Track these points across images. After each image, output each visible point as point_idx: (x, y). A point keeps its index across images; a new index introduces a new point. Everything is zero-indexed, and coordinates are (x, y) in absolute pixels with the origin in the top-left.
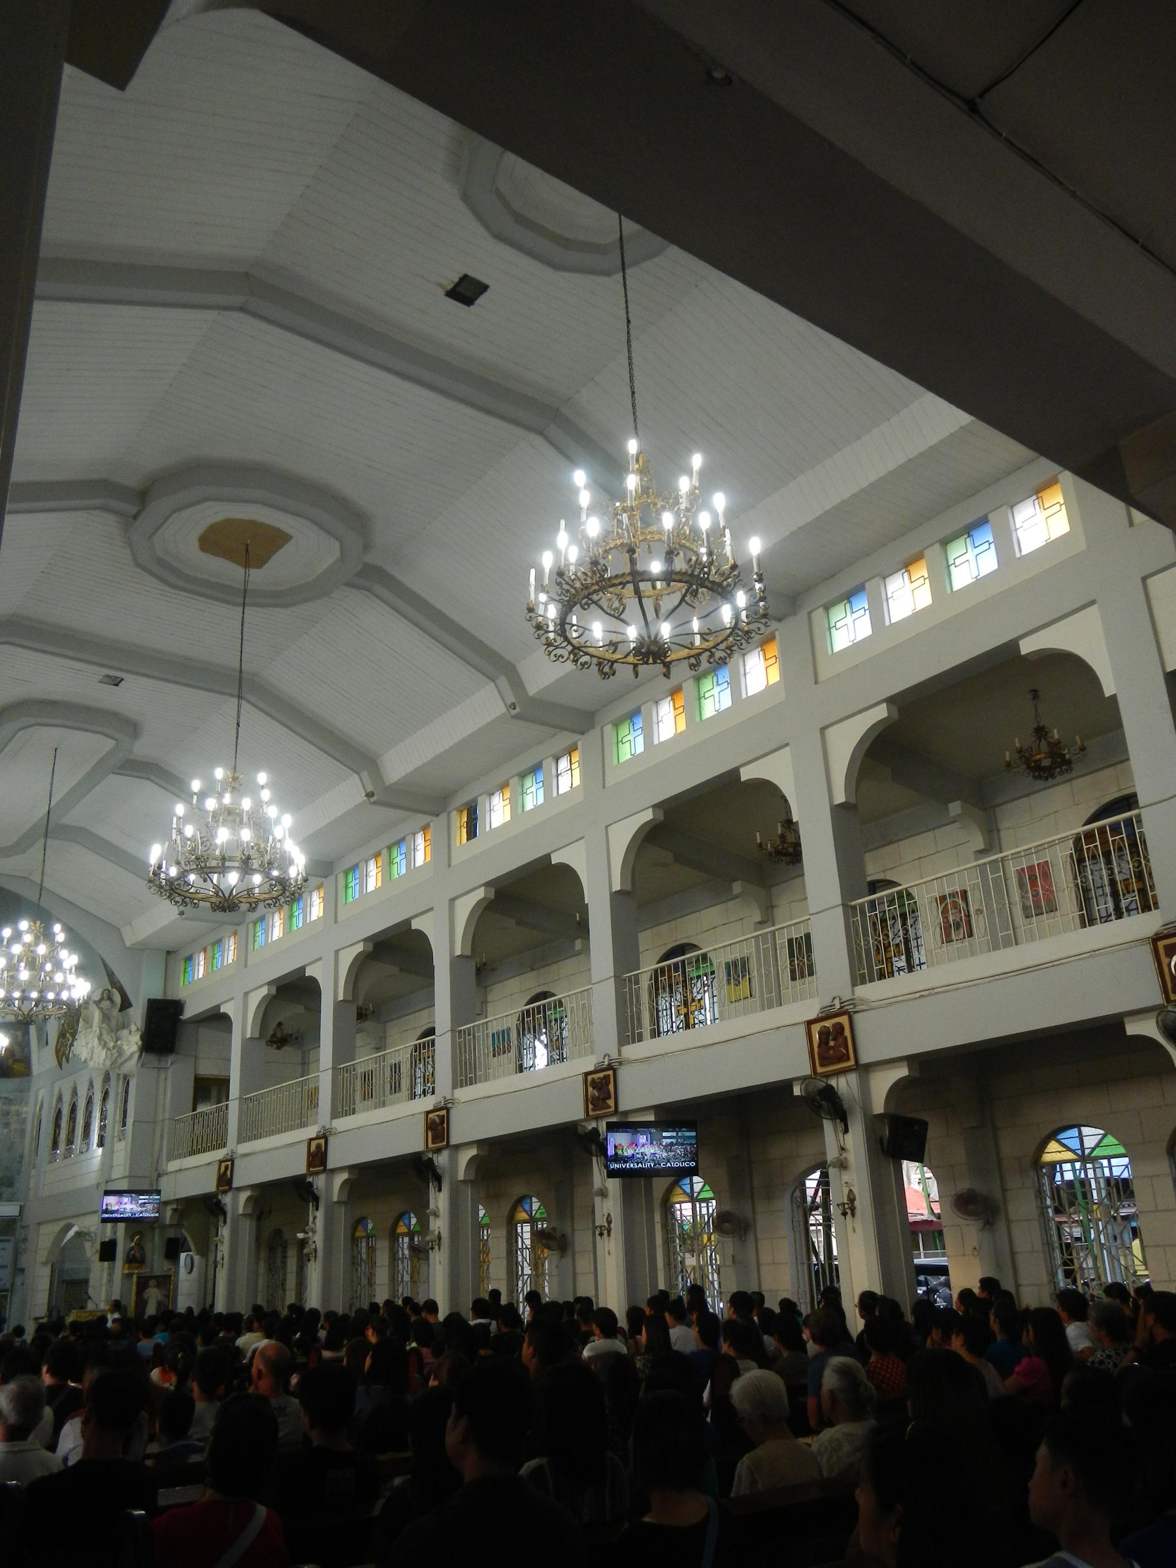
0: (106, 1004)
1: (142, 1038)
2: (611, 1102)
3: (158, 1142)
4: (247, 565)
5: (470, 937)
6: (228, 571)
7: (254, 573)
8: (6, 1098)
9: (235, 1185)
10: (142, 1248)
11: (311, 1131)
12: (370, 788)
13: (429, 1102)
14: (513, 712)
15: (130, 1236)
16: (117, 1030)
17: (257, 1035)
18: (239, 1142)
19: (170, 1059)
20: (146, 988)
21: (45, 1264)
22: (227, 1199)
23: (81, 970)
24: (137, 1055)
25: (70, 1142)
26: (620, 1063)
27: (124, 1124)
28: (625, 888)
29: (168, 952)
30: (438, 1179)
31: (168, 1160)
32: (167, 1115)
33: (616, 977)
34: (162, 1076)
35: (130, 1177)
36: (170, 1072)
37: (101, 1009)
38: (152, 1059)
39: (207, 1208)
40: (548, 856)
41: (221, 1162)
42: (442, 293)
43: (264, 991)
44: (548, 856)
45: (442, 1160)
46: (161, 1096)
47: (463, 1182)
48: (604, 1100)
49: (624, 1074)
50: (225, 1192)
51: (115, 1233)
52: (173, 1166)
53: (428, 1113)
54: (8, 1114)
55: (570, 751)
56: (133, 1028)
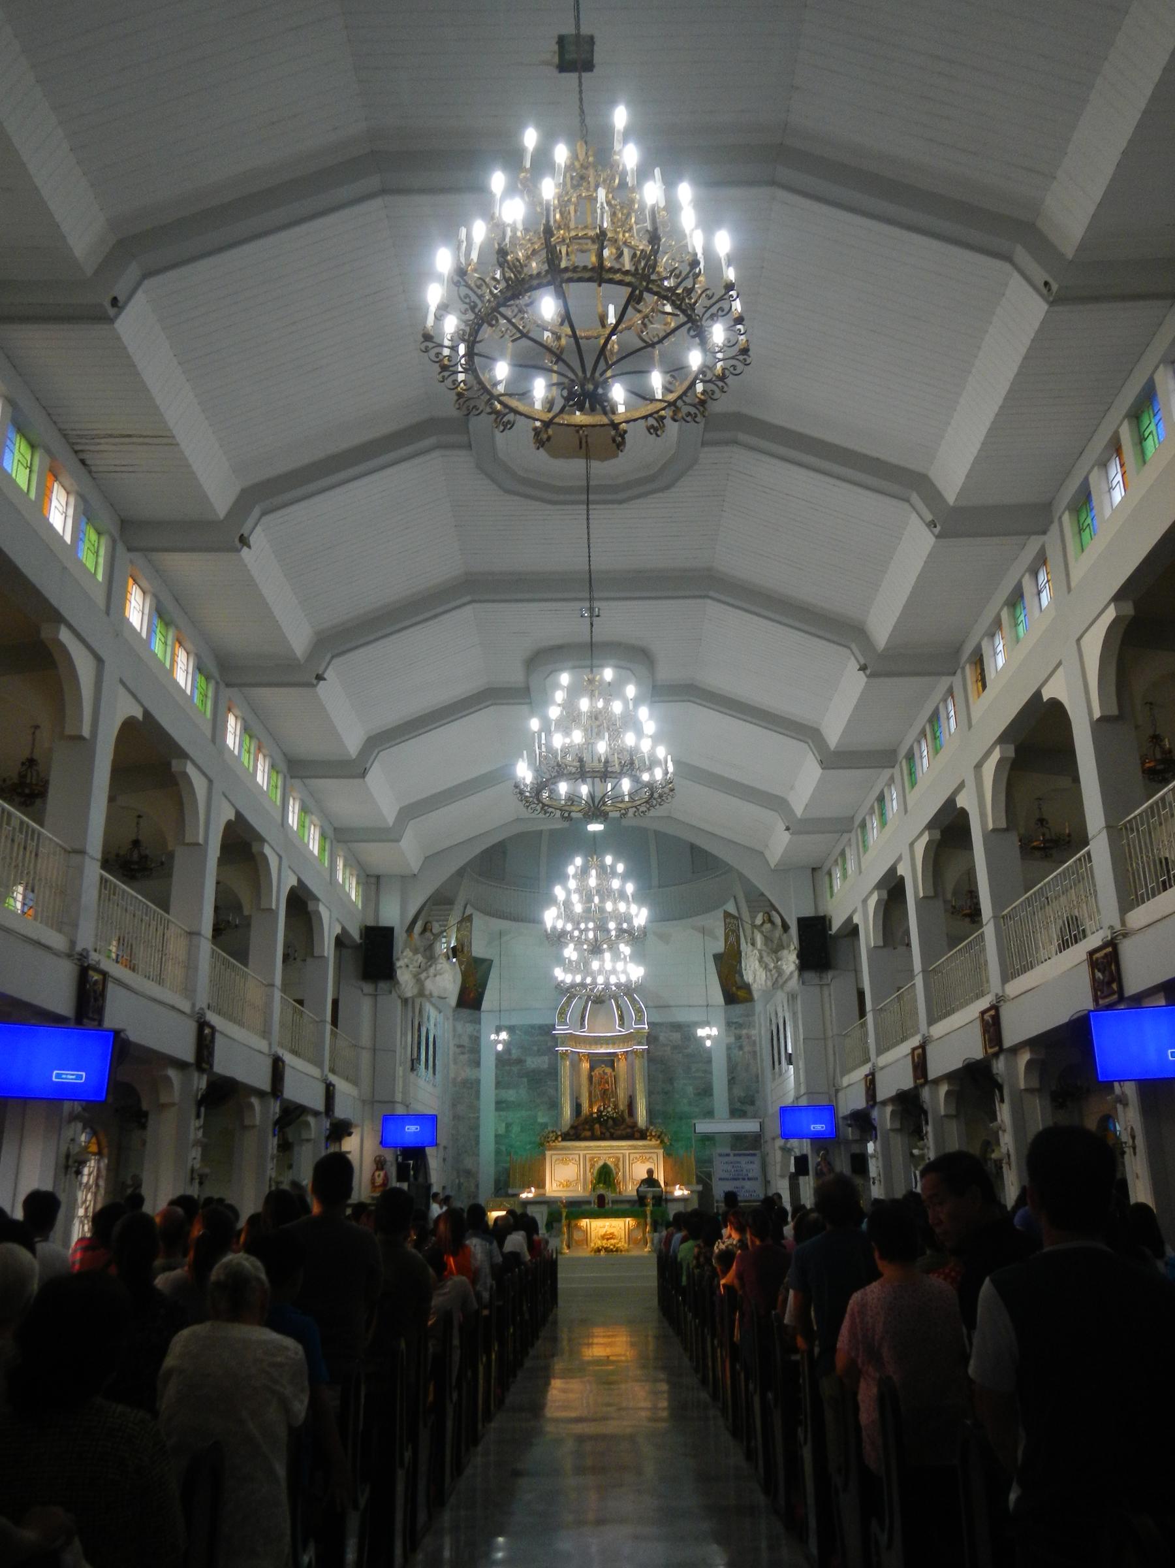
0: (768, 926)
1: (798, 957)
2: (1114, 986)
3: (831, 1058)
4: (588, 457)
5: (1003, 805)
6: (573, 468)
7: (595, 464)
10: (829, 1164)
11: (915, 1041)
12: (862, 661)
13: (984, 1003)
14: (937, 530)
15: (816, 1151)
16: (776, 951)
17: (881, 944)
19: (830, 974)
20: (795, 909)
21: (782, 1176)
22: (875, 1114)
23: (641, 897)
24: (796, 974)
25: (780, 1063)
26: (1125, 935)
28: (1107, 713)
29: (814, 869)
30: (1000, 1088)
31: (843, 1075)
33: (1109, 827)
34: (826, 993)
35: (808, 1093)
37: (762, 932)
38: (810, 975)
39: (862, 1121)
40: (1038, 694)
41: (867, 1076)
42: (555, 72)
43: (875, 897)
44: (1038, 694)
45: (1000, 1066)
46: (828, 1013)
47: (1026, 1090)
48: (1109, 983)
49: (1129, 951)
50: (873, 1106)
52: (845, 1081)
53: (983, 1013)
55: (1041, 560)
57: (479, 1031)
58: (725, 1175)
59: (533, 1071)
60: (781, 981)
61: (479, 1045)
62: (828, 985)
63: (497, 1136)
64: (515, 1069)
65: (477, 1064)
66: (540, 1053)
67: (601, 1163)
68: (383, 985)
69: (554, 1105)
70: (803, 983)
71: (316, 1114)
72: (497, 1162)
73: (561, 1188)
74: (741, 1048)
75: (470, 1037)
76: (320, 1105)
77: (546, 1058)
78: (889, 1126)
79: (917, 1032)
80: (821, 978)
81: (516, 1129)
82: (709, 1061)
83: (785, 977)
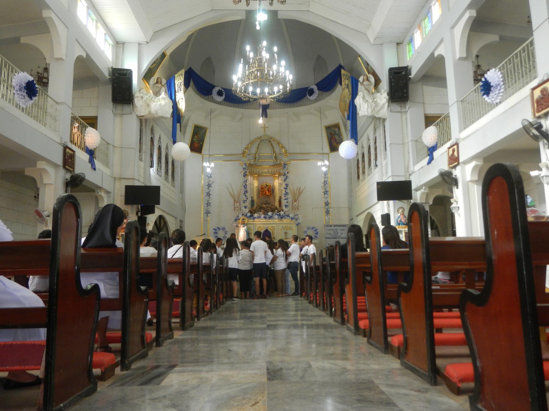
0: (366, 83)
1: (388, 94)
9: (461, 160)
18: (461, 131)
22: (457, 172)
24: (387, 104)
25: (364, 173)
27: (386, 150)
29: (398, 44)
31: (414, 165)
32: (410, 139)
35: (393, 176)
36: (408, 113)
38: (396, 107)
41: (449, 148)
50: (455, 167)
51: (389, 211)
52: (417, 167)
56: (383, 91)
58: (329, 236)
60: (377, 109)
62: (406, 112)
67: (265, 229)
68: (127, 108)
70: (391, 111)
71: (55, 166)
76: (60, 162)
78: (468, 178)
79: (535, 78)
80: (401, 106)
83: (379, 108)
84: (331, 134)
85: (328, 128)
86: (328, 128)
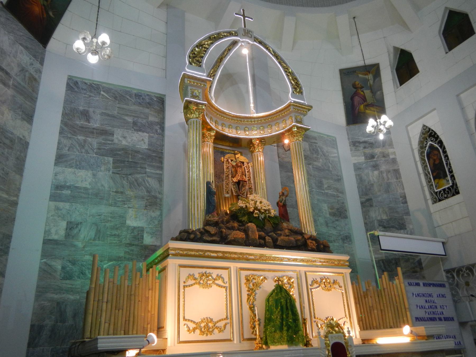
8: (365, 142)
54: (372, 157)
57: (39, 72)
59: (125, 150)
61: (35, 90)
63: (46, 242)
64: (94, 142)
65: (29, 117)
66: (137, 127)
67: (269, 286)
69: (154, 202)
72: (41, 291)
73: (197, 336)
74: (376, 167)
75: (23, 70)
77: (145, 136)
81: (86, 233)
82: (339, 179)
84: (354, 86)
85: (346, 74)
86: (346, 74)
